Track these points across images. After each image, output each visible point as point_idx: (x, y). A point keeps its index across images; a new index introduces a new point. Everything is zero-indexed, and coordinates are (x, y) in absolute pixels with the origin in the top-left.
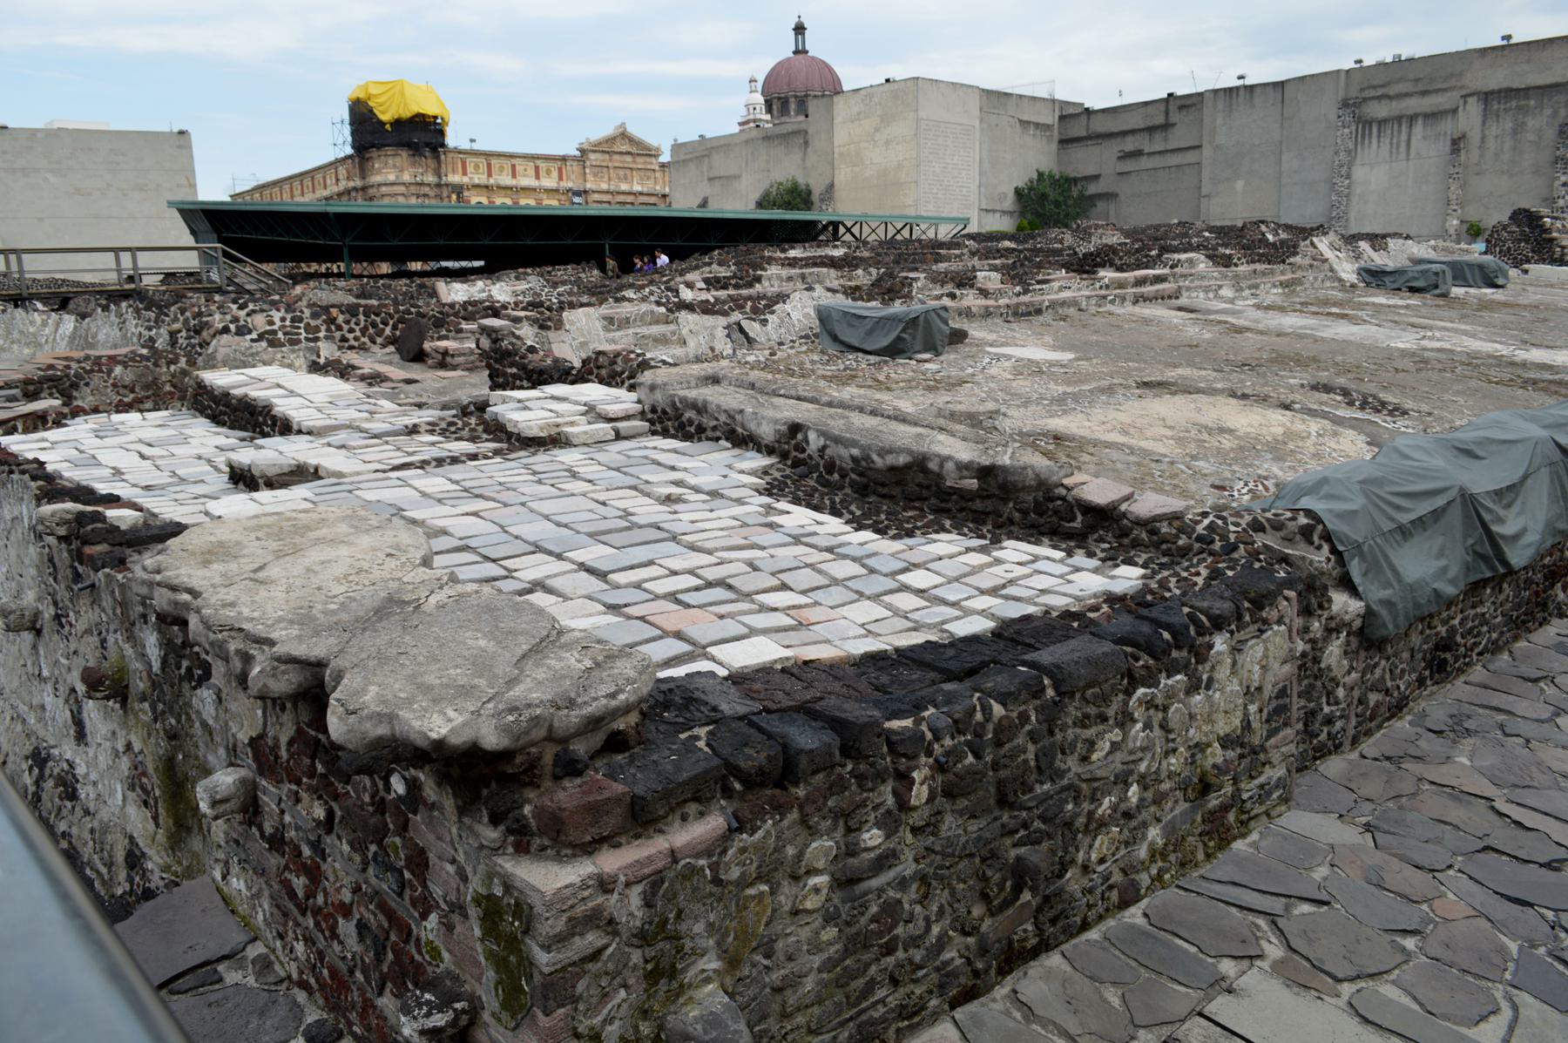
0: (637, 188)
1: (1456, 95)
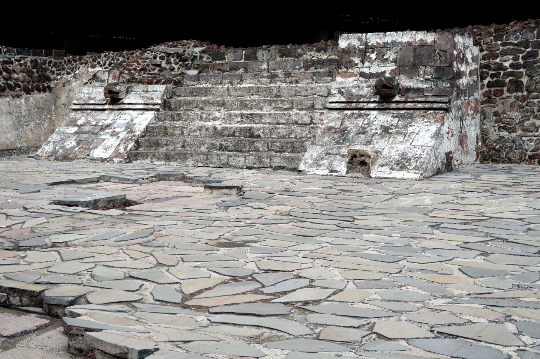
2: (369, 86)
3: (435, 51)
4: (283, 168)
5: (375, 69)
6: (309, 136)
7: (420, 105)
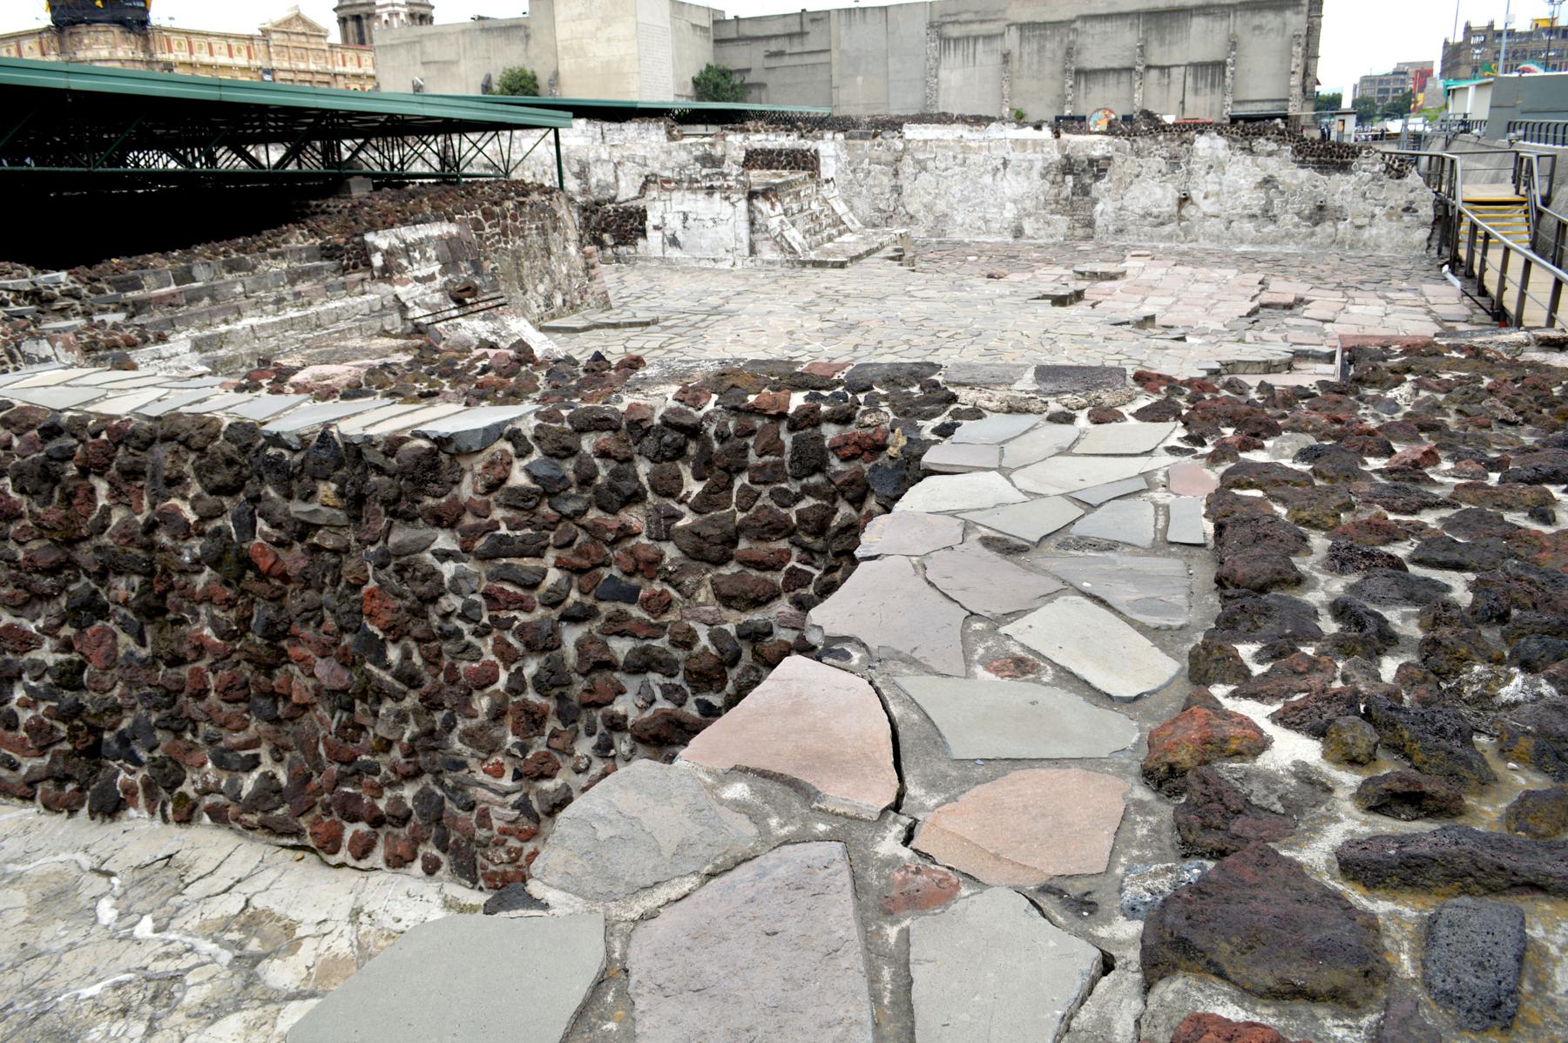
0: (313, 67)
1: (1002, 24)
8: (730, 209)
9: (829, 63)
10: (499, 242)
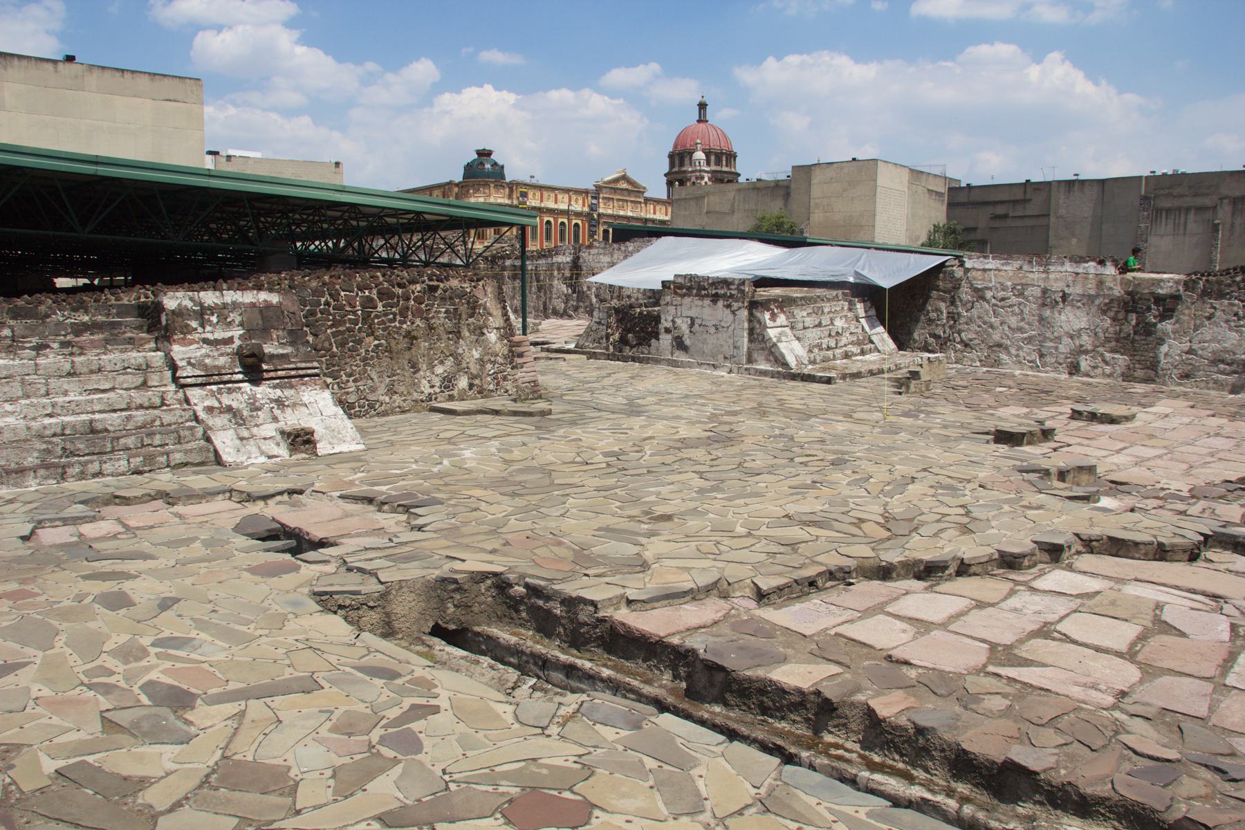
0: (630, 214)
2: (222, 355)
3: (283, 312)
4: (186, 464)
5: (220, 335)
6: (180, 421)
7: (293, 373)
8: (731, 317)
9: (1048, 226)
10: (394, 320)
